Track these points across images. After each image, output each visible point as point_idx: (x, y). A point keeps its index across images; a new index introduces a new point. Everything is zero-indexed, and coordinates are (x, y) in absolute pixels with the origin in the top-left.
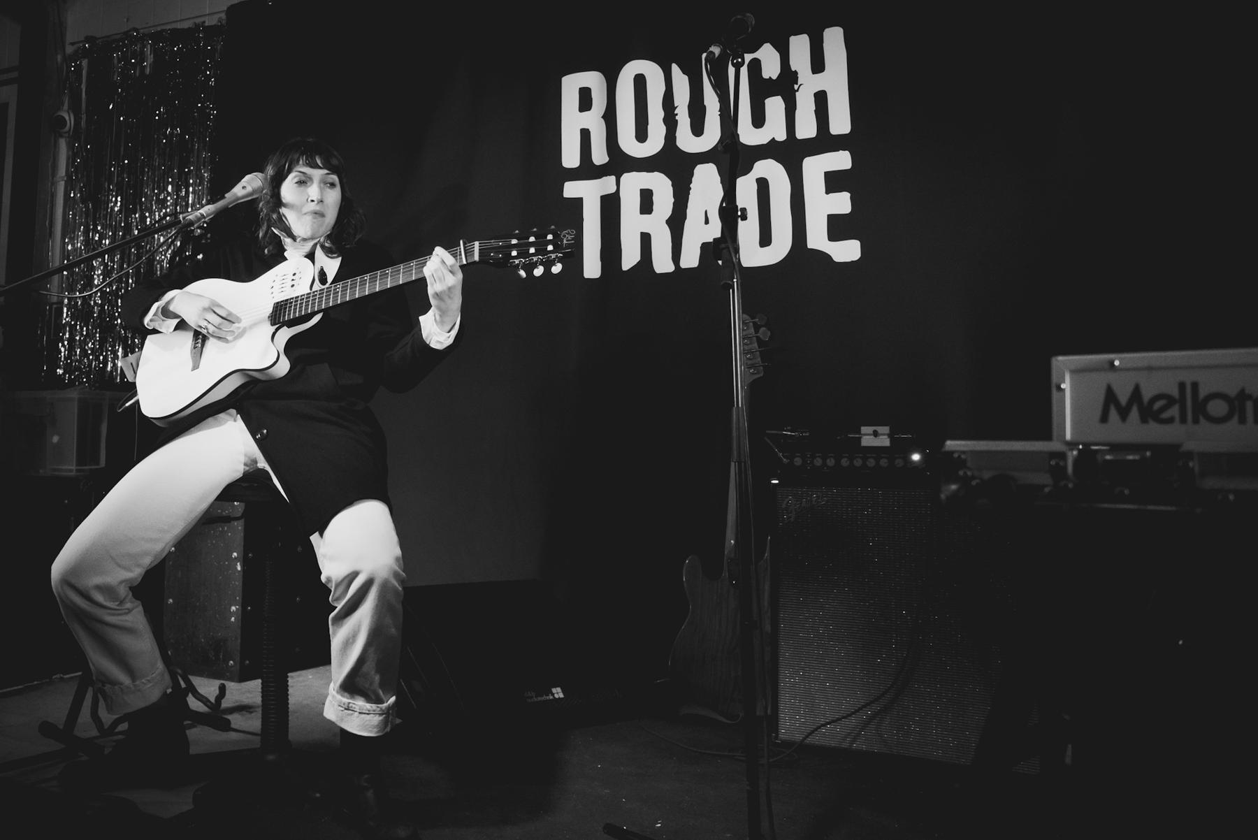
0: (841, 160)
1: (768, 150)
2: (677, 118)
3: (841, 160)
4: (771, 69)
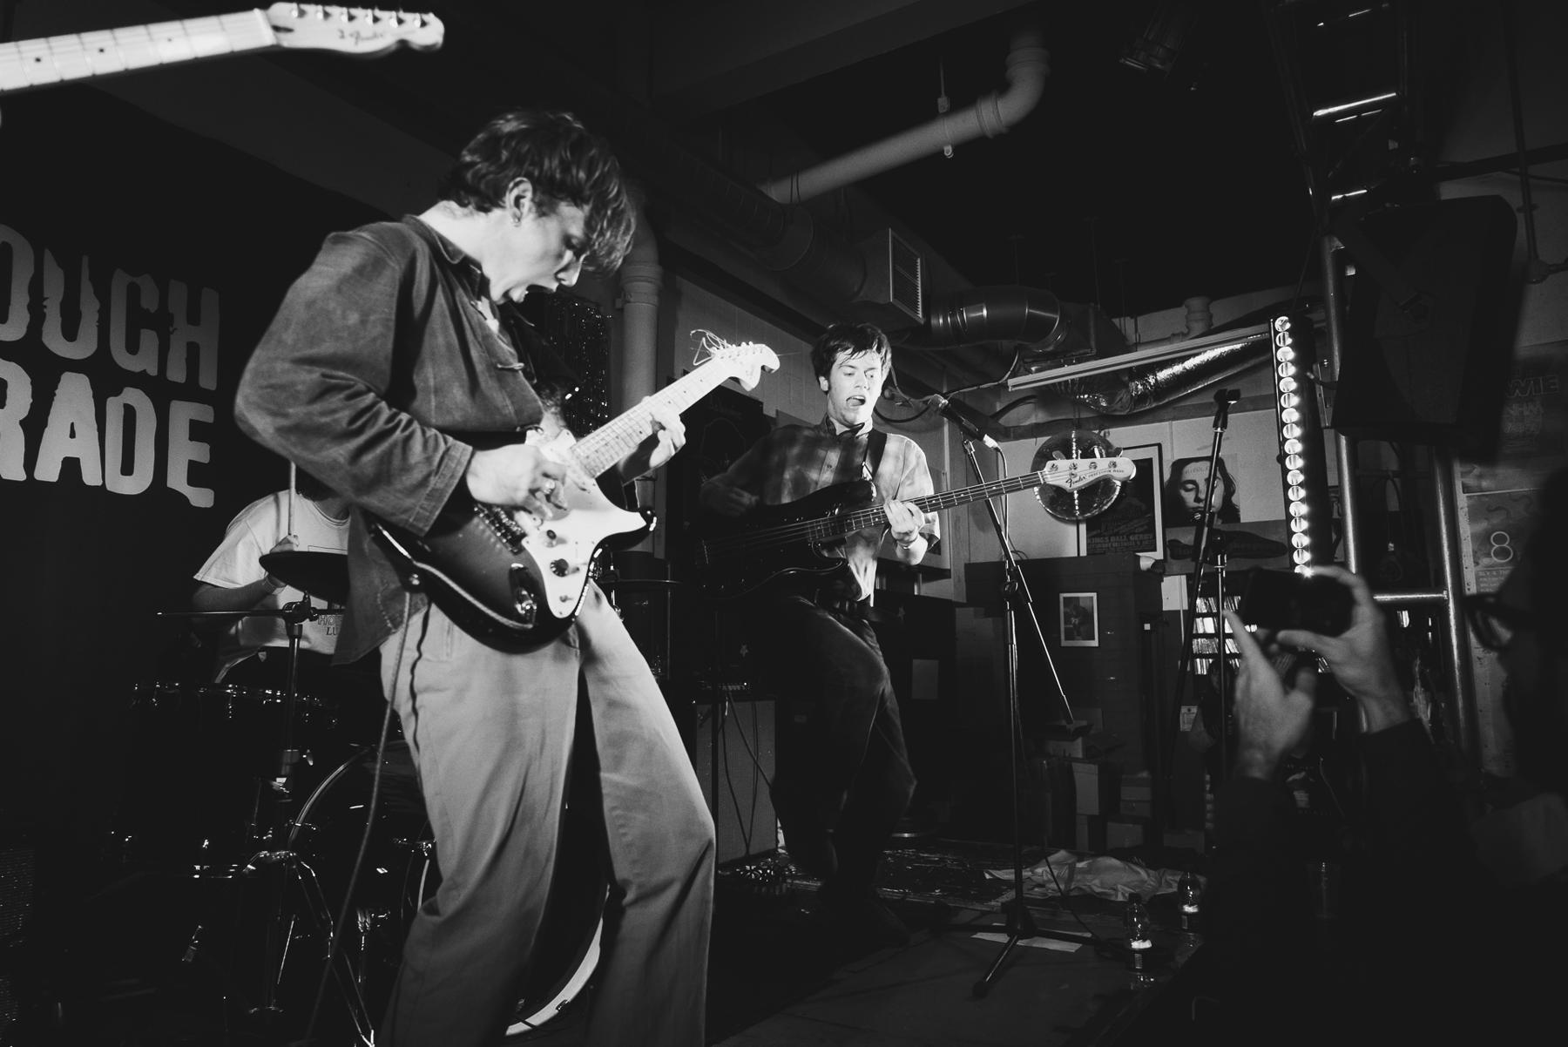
0: (205, 413)
1: (139, 380)
2: (45, 310)
3: (205, 413)
4: (149, 302)
